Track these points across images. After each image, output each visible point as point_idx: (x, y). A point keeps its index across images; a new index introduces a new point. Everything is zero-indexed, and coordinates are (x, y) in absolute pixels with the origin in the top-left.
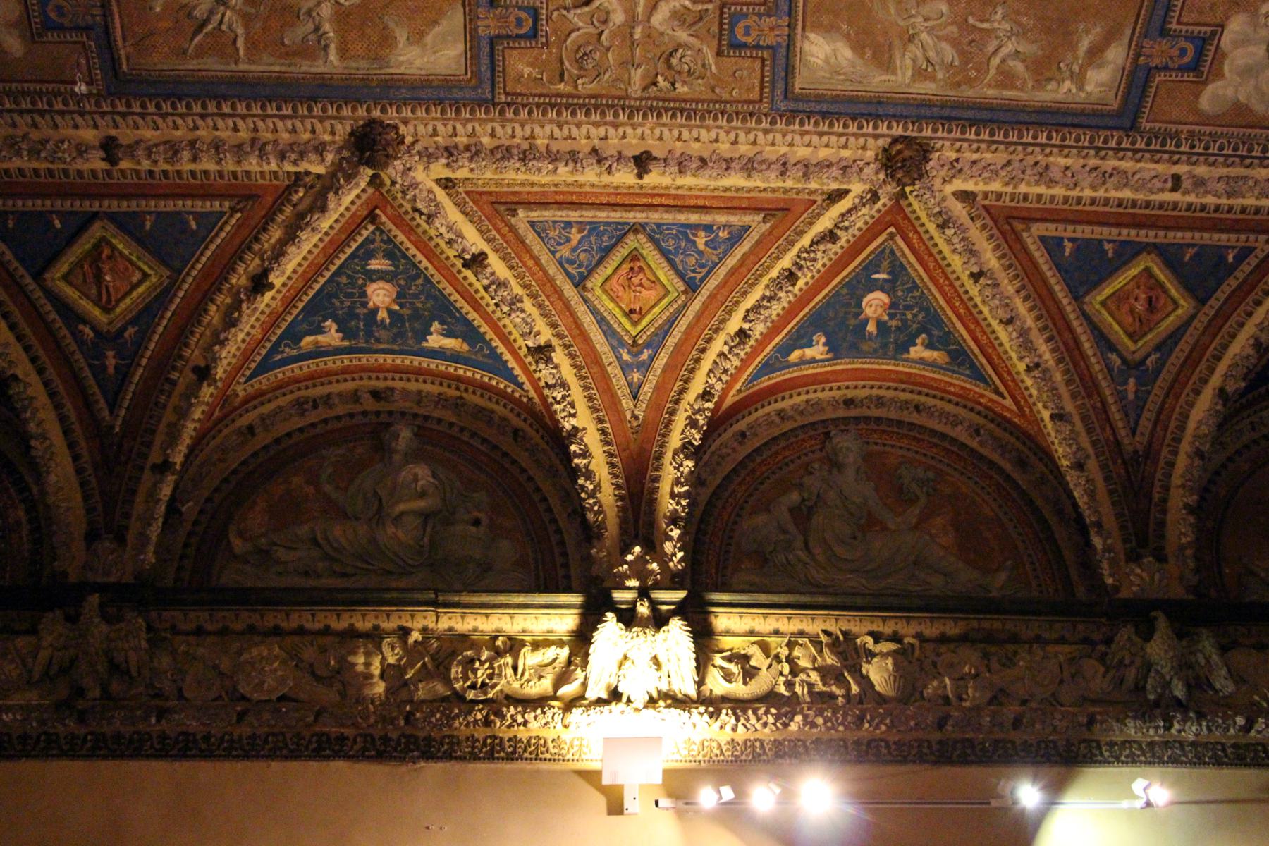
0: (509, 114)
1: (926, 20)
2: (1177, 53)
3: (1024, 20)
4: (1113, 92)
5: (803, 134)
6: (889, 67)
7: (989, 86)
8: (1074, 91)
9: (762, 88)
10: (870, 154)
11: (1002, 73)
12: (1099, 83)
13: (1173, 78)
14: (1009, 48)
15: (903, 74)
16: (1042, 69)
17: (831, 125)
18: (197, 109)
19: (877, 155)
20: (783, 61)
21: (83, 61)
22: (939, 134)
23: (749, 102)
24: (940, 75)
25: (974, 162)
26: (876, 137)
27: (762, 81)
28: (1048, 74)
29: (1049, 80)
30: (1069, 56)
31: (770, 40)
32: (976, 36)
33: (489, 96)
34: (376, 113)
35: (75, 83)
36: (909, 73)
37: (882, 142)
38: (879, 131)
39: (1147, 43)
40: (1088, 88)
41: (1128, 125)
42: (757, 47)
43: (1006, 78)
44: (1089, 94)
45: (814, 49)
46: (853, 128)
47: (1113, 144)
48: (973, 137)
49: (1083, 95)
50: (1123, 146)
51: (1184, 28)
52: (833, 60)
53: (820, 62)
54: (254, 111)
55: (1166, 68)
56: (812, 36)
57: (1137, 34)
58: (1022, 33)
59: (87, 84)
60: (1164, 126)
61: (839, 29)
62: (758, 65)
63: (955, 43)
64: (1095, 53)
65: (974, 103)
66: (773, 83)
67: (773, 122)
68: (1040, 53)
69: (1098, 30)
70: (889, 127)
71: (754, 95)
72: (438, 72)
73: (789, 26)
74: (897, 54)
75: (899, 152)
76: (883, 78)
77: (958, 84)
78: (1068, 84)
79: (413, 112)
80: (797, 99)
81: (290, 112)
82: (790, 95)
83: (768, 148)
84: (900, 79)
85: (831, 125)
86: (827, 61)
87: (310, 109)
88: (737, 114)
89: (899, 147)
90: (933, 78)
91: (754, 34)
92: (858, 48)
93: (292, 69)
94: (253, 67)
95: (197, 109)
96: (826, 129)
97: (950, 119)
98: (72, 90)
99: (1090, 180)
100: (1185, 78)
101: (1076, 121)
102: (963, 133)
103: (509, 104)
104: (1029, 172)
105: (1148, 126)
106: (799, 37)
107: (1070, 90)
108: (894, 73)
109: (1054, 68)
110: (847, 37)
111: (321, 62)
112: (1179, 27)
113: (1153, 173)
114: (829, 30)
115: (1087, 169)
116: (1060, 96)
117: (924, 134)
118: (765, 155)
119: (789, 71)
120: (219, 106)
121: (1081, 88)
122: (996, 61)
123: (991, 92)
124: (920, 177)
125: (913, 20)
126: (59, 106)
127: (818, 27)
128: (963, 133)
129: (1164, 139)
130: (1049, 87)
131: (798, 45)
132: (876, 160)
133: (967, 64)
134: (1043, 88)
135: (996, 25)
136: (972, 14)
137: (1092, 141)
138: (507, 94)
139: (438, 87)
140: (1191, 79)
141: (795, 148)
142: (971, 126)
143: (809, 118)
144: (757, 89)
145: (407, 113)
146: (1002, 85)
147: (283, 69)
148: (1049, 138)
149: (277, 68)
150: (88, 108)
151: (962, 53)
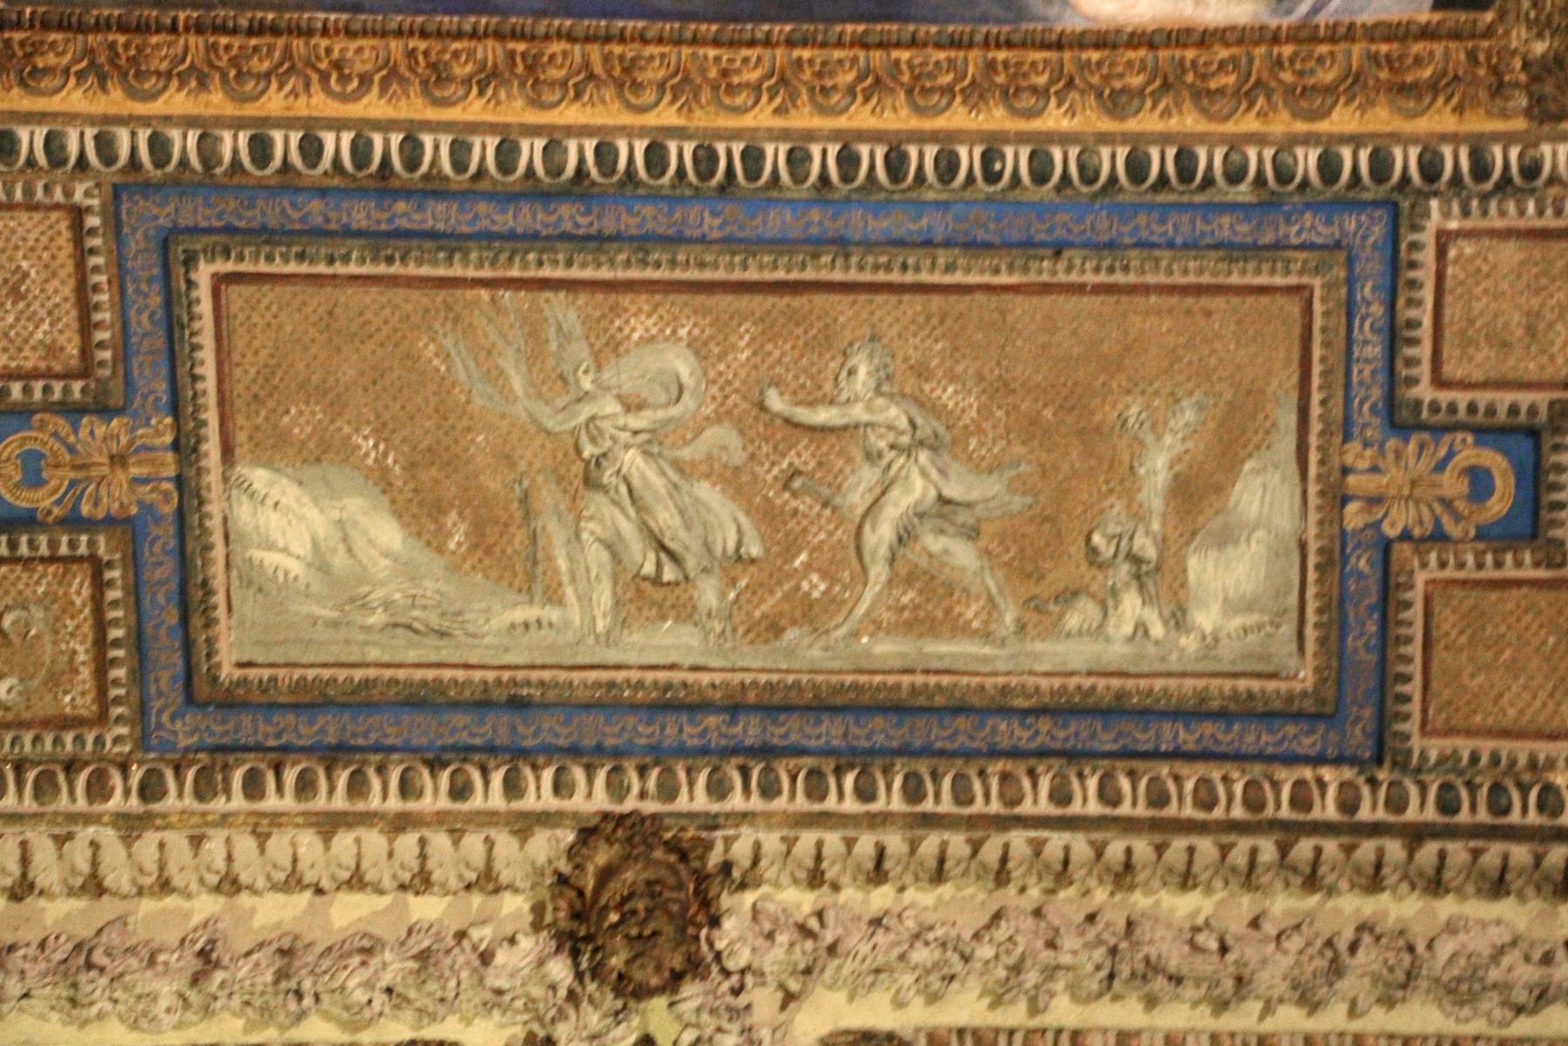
1: (632, 405)
2: (1463, 486)
3: (947, 395)
4: (1288, 629)
5: (263, 828)
6: (530, 575)
7: (876, 627)
8: (1157, 630)
9: (102, 667)
10: (515, 906)
11: (909, 581)
12: (1229, 595)
13: (1469, 573)
14: (915, 488)
15: (585, 600)
16: (1045, 556)
17: (357, 787)
19: (538, 909)
20: (167, 570)
22: (736, 801)
23: (64, 723)
24: (708, 594)
25: (876, 922)
26: (524, 824)
27: (101, 643)
28: (1059, 577)
29: (1069, 596)
30: (1117, 507)
31: (116, 495)
32: (802, 456)
36: (604, 597)
37: (547, 846)
38: (529, 802)
39: (1354, 454)
40: (1205, 619)
41: (1358, 737)
42: (74, 522)
43: (929, 601)
44: (1212, 642)
45: (272, 522)
46: (434, 797)
47: (1327, 809)
48: (851, 805)
49: (1189, 643)
50: (1364, 814)
51: (1462, 398)
52: (339, 560)
53: (295, 567)
55: (1438, 537)
56: (259, 477)
57: (1316, 427)
58: (939, 440)
60: (1486, 746)
61: (346, 453)
62: (79, 589)
63: (734, 482)
64: (1196, 494)
65: (840, 689)
66: (139, 641)
67: (151, 789)
68: (1018, 502)
69: (1189, 415)
70: (561, 787)
71: (77, 698)
73: (176, 446)
74: (555, 532)
75: (607, 874)
76: (520, 614)
77: (775, 628)
78: (1131, 605)
80: (230, 701)
82: (202, 689)
83: (147, 905)
84: (570, 621)
85: (357, 787)
86: (319, 563)
88: (19, 768)
89: (602, 855)
90: (686, 612)
91: (58, 479)
92: (421, 510)
96: (340, 802)
97: (766, 752)
99: (1285, 962)
100: (1509, 572)
101: (1187, 738)
102: (816, 791)
104: (1069, 942)
105: (1435, 748)
106: (213, 478)
107: (1141, 628)
108: (553, 596)
109: (1077, 550)
110: (381, 479)
112: (1445, 397)
113: (1499, 935)
114: (316, 455)
115: (1270, 929)
116: (1116, 651)
117: (682, 803)
118: (139, 932)
119: (192, 600)
121: (1178, 619)
122: (880, 536)
123: (886, 649)
124: (694, 967)
125: (586, 411)
127: (275, 447)
128: (816, 791)
129: (1497, 789)
130: (1073, 621)
131: (214, 508)
132: (537, 926)
133: (790, 551)
134: (1054, 629)
135: (858, 413)
136: (776, 382)
137: (1254, 802)
140: (1529, 573)
141: (245, 899)
142: (839, 772)
143: (278, 769)
144: (85, 673)
146: (916, 624)
148: (1109, 795)
151: (768, 516)
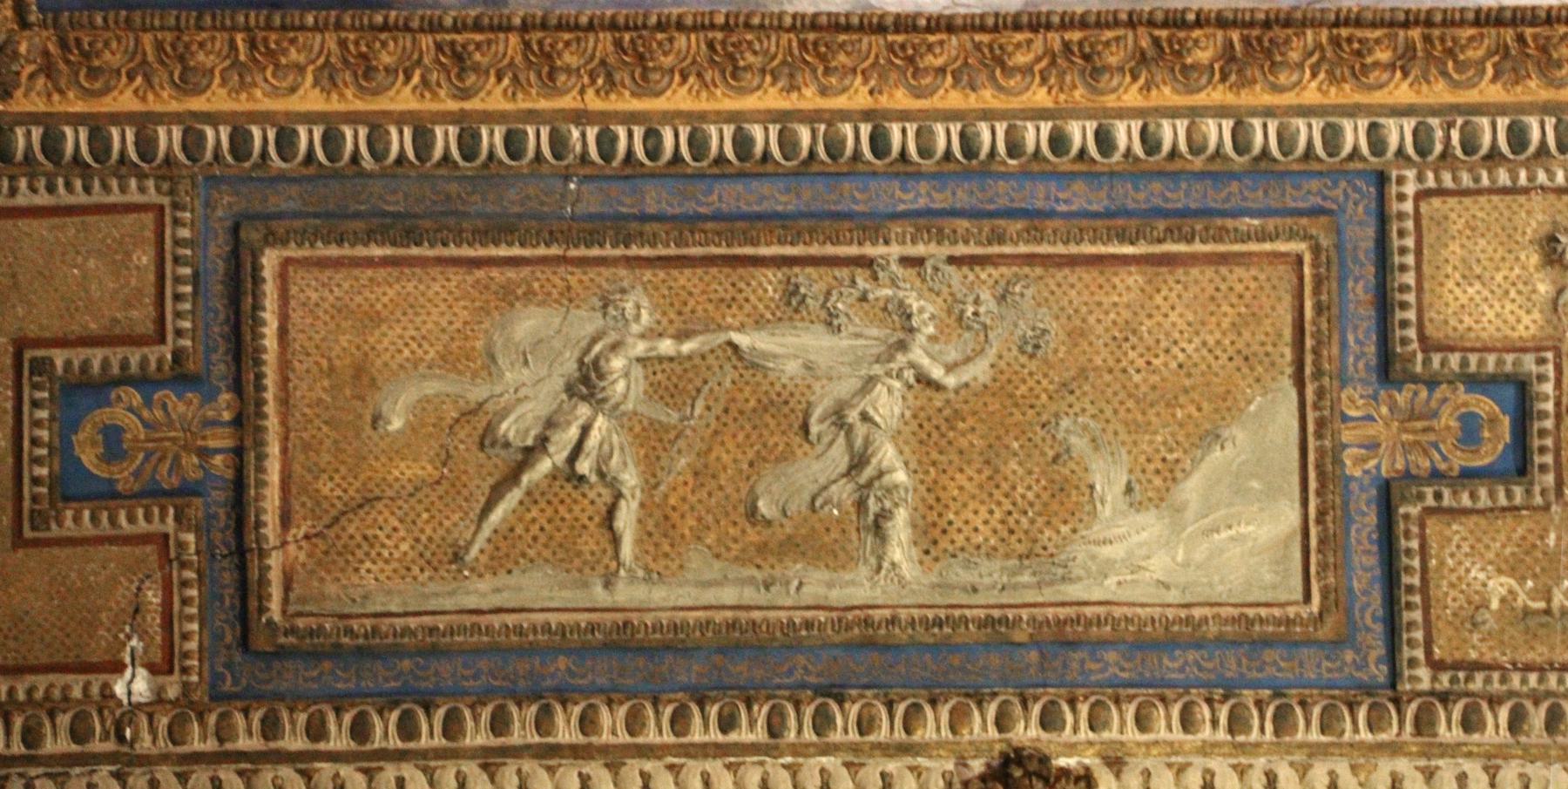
0: (1448, 731)
18: (477, 736)
21: (153, 597)
33: (1380, 673)
34: (1027, 732)
35: (118, 668)
54: (651, 736)
59: (153, 669)
72: (1220, 592)
79: (1142, 723)
81: (760, 735)
87: (823, 722)
93: (777, 596)
94: (659, 595)
95: (477, 736)
98: (107, 694)
103: (1445, 698)
111: (864, 571)
120: (543, 722)
126: (56, 743)
138: (1437, 666)
139: (1220, 641)
145: (1121, 729)
147: (750, 595)
149: (729, 595)
150: (145, 744)
